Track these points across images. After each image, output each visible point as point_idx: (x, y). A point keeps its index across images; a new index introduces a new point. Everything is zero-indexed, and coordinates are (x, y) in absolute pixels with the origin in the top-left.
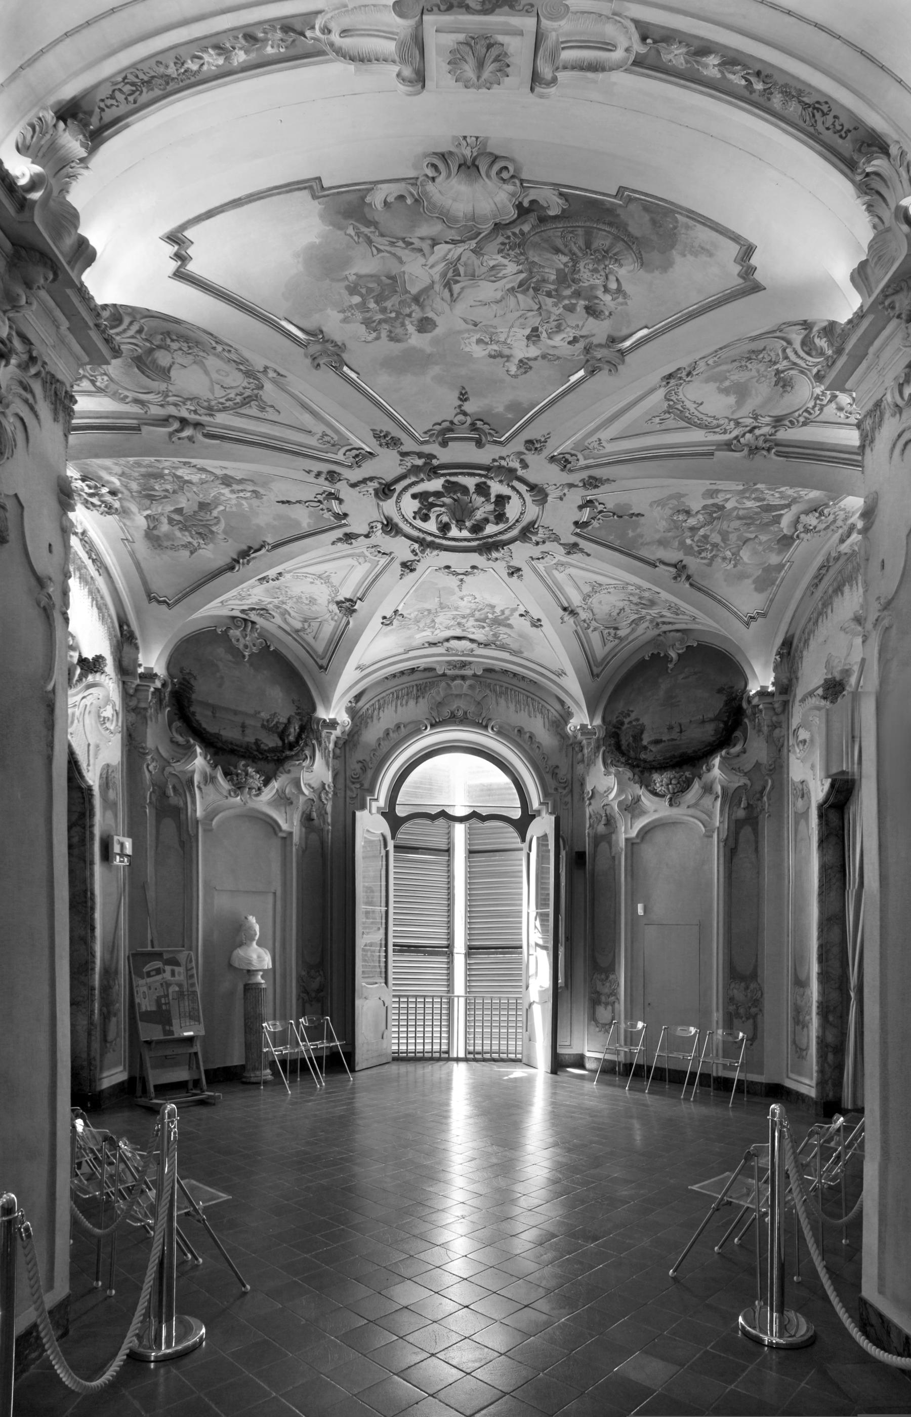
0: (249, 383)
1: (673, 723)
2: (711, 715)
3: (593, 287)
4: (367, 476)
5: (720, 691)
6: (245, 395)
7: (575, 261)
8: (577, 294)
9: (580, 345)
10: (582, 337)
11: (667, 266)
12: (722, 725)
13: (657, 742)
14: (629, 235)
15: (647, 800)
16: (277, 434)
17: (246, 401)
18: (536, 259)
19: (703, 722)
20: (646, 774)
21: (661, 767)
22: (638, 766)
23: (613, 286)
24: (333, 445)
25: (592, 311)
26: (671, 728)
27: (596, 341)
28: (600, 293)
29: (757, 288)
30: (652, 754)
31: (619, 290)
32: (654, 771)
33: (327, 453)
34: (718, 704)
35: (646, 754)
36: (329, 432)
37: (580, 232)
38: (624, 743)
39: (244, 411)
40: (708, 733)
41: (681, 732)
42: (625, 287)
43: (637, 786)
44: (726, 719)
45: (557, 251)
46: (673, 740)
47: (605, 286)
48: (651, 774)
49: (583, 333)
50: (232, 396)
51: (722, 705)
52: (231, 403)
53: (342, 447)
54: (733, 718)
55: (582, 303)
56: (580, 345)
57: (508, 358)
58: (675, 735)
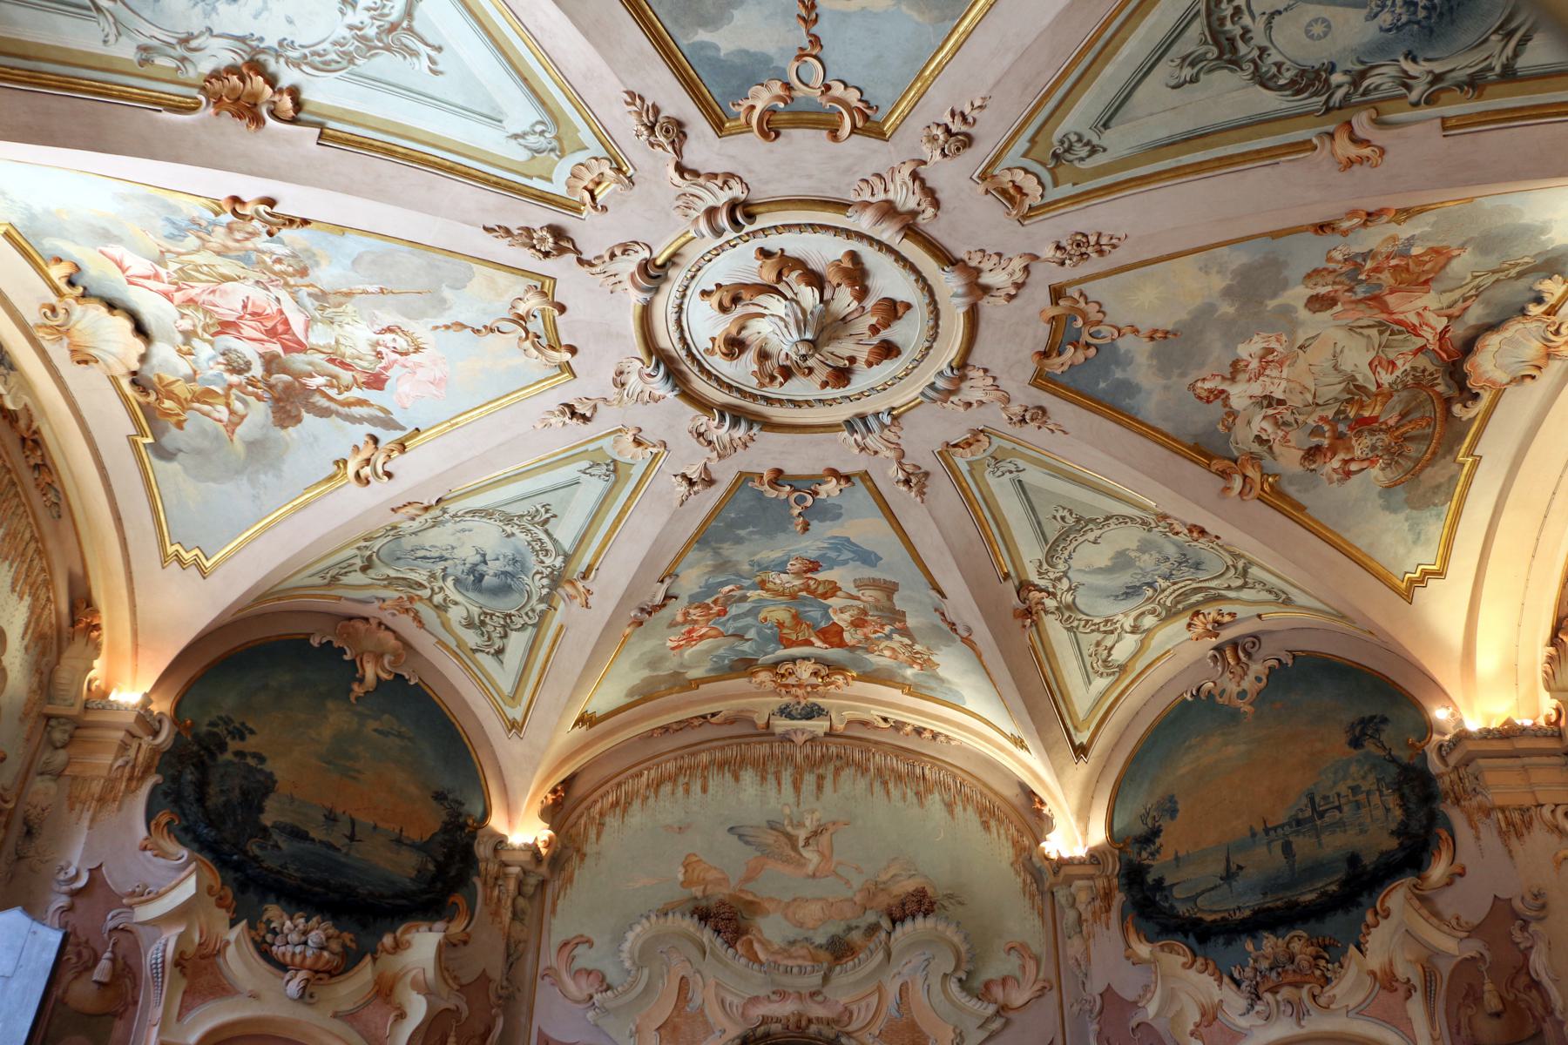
0: (1279, 65)
1: (339, 811)
2: (413, 834)
3: (1350, 449)
4: (939, 195)
5: (440, 797)
6: (1240, 44)
7: (1389, 430)
8: (1339, 436)
9: (1256, 448)
10: (1270, 448)
11: (1390, 508)
12: (431, 867)
13: (297, 834)
14: (1421, 470)
15: (239, 960)
16: (1109, 70)
17: (1216, 34)
18: (1395, 398)
19: (399, 841)
20: (252, 896)
21: (301, 898)
22: (237, 867)
23: (1353, 467)
24: (1055, 155)
25: (1312, 453)
26: (331, 818)
27: (1267, 461)
28: (1342, 456)
29: (1408, 596)
30: (276, 855)
31: (1349, 474)
32: (272, 897)
33: (1033, 141)
34: (431, 821)
35: (262, 848)
36: (1100, 159)
37: (1428, 431)
38: (215, 800)
39: (1197, 28)
40: (404, 867)
41: (352, 838)
42: (1354, 478)
43: (223, 916)
44: (441, 859)
45: (1403, 416)
46: (330, 846)
47: (1352, 460)
48: (263, 900)
49: (1276, 448)
50: (1246, 20)
51: (437, 827)
52: (1229, 12)
53: (1052, 171)
54: (450, 867)
55: (1326, 443)
56: (1256, 448)
57: (1233, 379)
58: (337, 837)
